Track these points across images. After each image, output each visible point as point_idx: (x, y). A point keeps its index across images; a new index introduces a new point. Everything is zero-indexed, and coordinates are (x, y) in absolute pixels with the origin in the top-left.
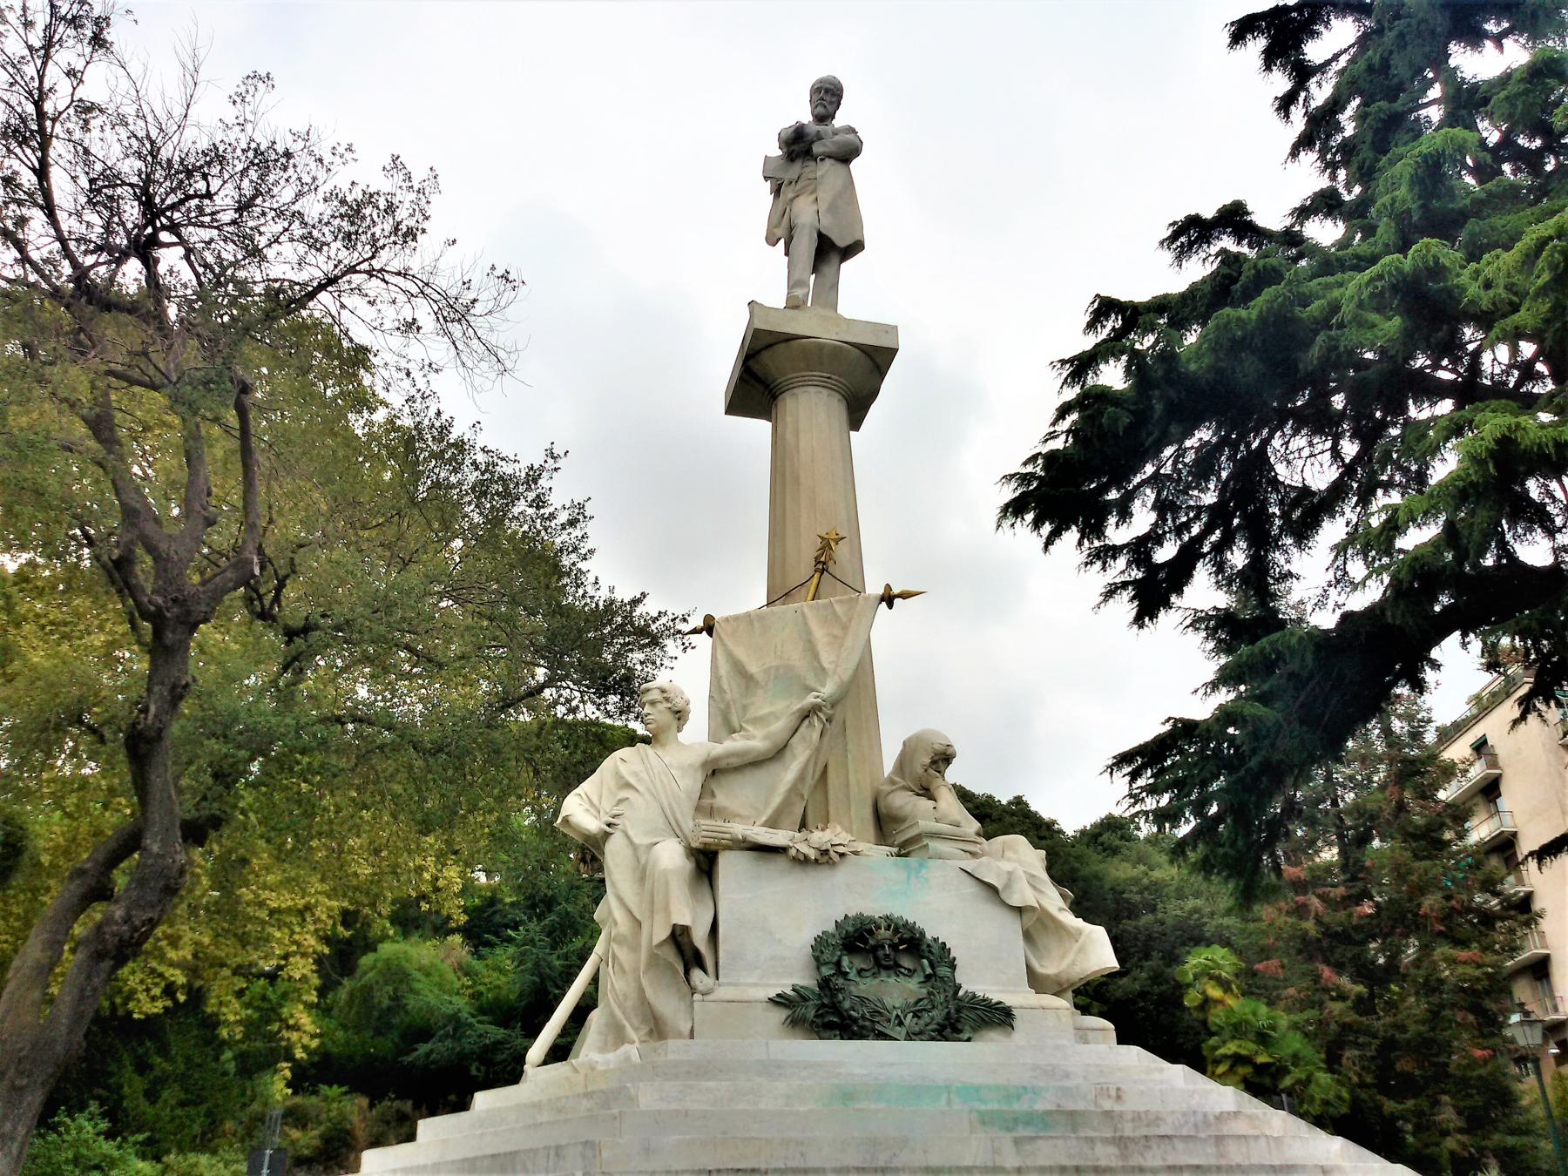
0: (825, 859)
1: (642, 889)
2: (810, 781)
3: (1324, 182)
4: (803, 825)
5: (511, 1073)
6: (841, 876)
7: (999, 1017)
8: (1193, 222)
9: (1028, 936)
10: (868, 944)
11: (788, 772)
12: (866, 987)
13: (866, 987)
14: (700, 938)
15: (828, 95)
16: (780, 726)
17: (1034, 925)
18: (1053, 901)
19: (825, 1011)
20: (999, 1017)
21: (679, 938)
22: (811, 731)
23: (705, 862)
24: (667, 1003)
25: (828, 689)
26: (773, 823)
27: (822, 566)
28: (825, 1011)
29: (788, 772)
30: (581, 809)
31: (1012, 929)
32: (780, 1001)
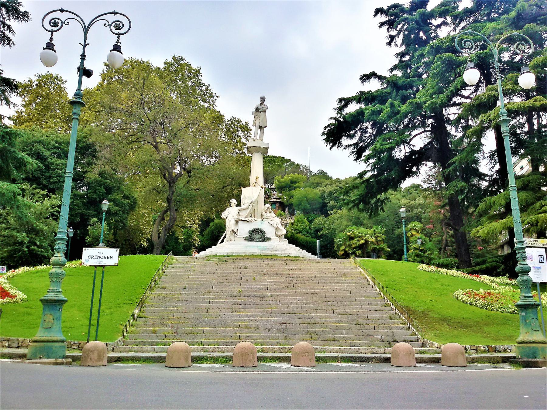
0: (251, 222)
1: (230, 225)
2: (252, 211)
3: (336, 115)
4: (251, 217)
5: (216, 245)
6: (253, 223)
7: (270, 239)
8: (365, 75)
9: (276, 230)
10: (254, 231)
11: (248, 210)
12: (254, 236)
13: (254, 236)
14: (235, 231)
15: (263, 99)
16: (248, 204)
17: (277, 229)
18: (280, 226)
19: (249, 239)
20: (270, 239)
21: (233, 231)
22: (251, 206)
23: (237, 222)
24: (232, 238)
25: (253, 200)
26: (246, 217)
27: (256, 181)
28: (249, 239)
29: (248, 210)
30: (224, 215)
31: (274, 229)
32: (244, 238)
